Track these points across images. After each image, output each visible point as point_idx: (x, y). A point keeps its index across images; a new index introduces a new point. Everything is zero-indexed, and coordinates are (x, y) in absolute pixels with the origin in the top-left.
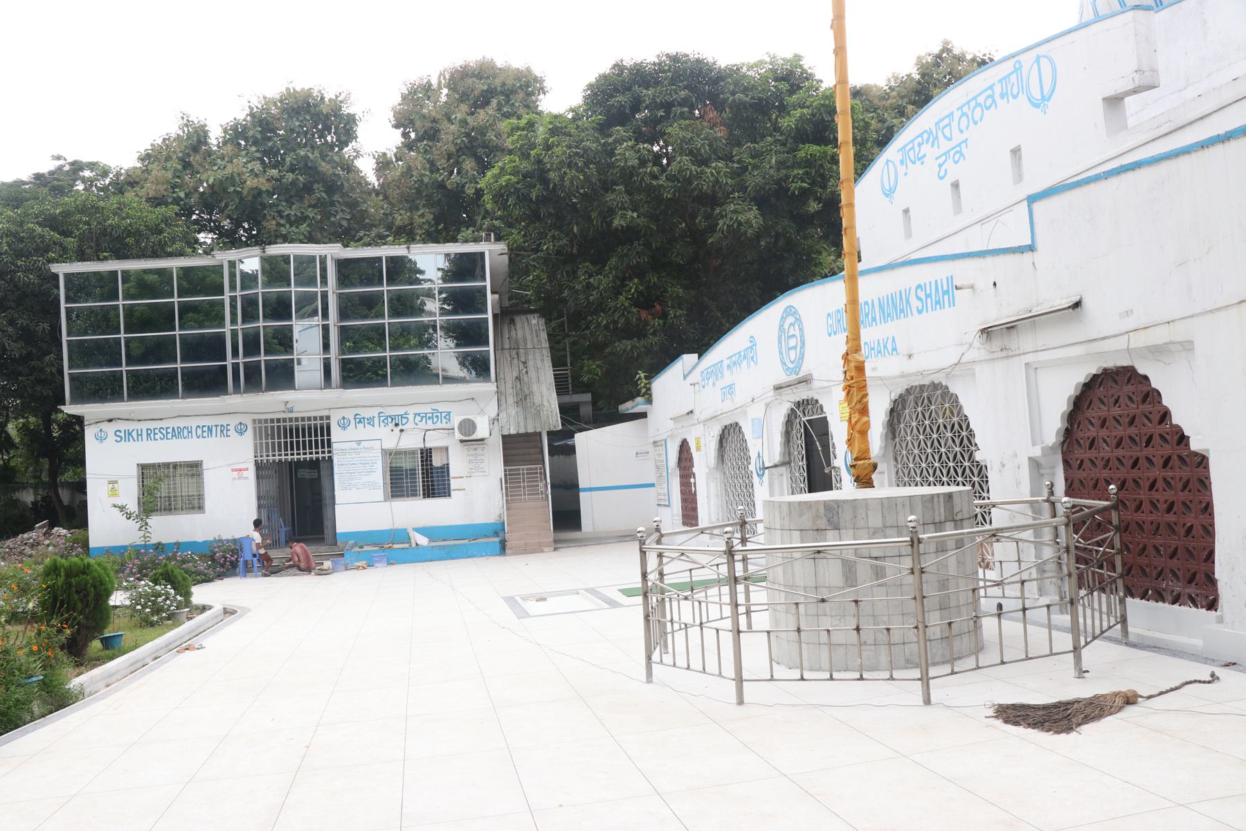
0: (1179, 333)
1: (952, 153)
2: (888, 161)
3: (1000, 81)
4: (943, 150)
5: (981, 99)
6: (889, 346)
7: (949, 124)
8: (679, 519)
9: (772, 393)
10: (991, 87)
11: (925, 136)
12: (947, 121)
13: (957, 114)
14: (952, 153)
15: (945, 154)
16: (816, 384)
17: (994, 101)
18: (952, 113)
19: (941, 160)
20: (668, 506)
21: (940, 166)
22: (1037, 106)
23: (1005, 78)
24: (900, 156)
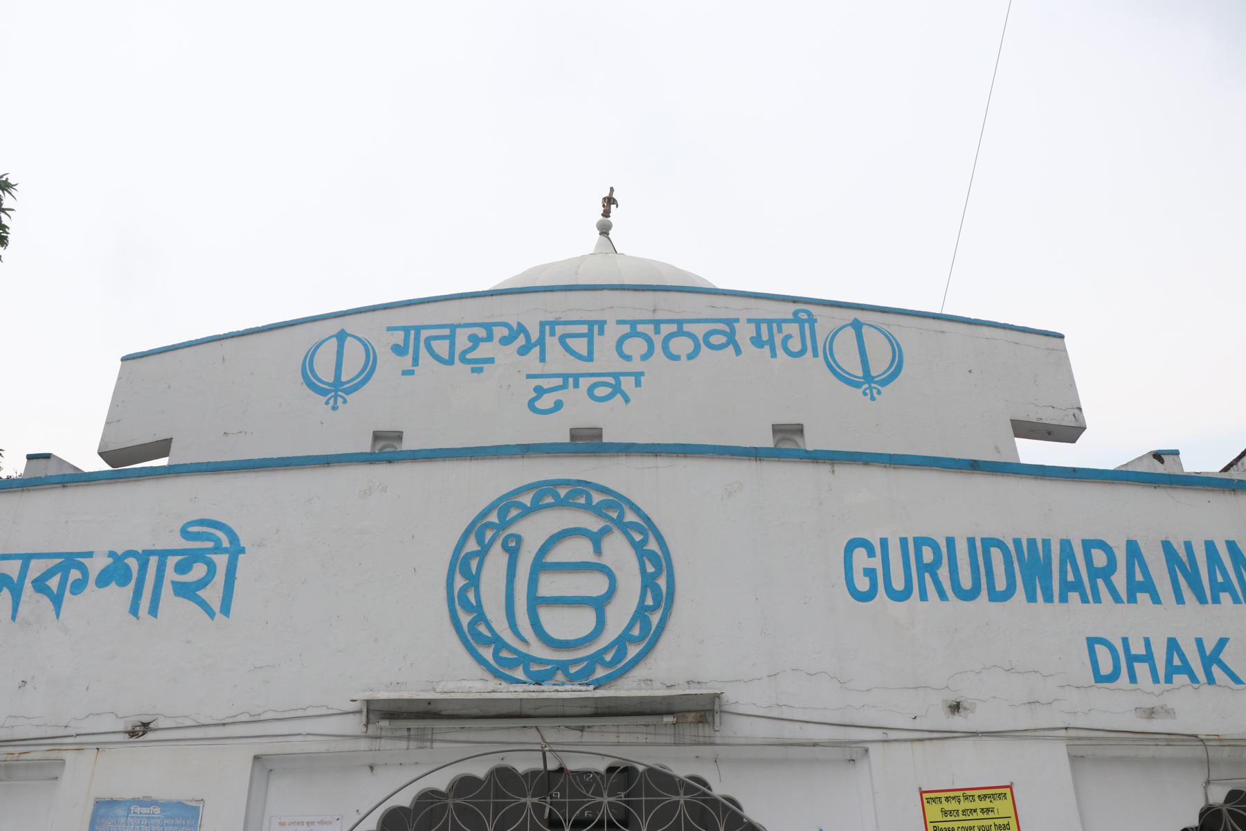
1: (585, 383)
2: (342, 336)
3: (758, 323)
4: (550, 368)
5: (699, 330)
7: (589, 336)
9: (354, 725)
10: (730, 322)
11: (500, 332)
12: (584, 329)
13: (614, 331)
15: (565, 377)
17: (731, 340)
18: (602, 324)
19: (546, 383)
21: (540, 391)
22: (857, 385)
23: (769, 322)
24: (399, 338)
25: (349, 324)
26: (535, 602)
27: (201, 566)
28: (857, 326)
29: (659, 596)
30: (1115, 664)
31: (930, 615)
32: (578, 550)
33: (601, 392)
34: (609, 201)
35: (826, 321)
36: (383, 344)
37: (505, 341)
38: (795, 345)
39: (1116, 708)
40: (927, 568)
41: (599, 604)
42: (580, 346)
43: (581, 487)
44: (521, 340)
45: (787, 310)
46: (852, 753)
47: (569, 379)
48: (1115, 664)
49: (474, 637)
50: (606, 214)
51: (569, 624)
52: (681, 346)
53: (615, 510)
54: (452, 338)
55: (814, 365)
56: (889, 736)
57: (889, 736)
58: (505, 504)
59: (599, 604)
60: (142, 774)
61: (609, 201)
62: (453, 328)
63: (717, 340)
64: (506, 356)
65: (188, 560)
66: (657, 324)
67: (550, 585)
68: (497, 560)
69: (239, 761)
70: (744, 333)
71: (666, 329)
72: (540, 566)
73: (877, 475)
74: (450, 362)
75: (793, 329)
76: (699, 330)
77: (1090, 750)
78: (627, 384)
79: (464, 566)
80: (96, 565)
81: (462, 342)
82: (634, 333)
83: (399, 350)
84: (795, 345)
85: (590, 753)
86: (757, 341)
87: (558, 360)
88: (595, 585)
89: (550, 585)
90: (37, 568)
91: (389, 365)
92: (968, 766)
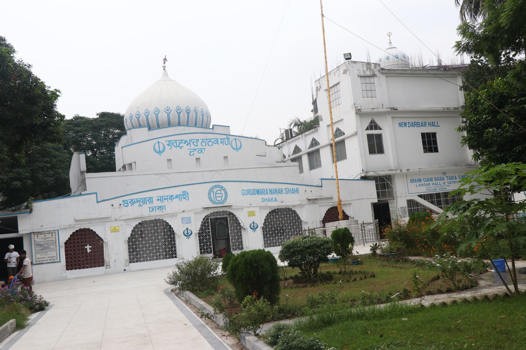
0: (350, 202)
1: (197, 150)
2: (158, 142)
3: (221, 139)
5: (213, 141)
6: (274, 199)
8: (65, 267)
10: (217, 139)
11: (183, 142)
13: (200, 141)
14: (197, 150)
16: (233, 207)
17: (217, 142)
19: (191, 150)
20: (60, 262)
21: (191, 152)
24: (168, 143)
25: (159, 140)
26: (216, 197)
27: (185, 195)
28: (235, 139)
29: (226, 196)
30: (264, 200)
31: (249, 196)
32: (219, 192)
33: (200, 152)
34: (165, 60)
35: (231, 138)
36: (166, 144)
37: (184, 143)
38: (227, 143)
39: (263, 204)
40: (249, 192)
41: (221, 197)
42: (195, 144)
43: (219, 186)
44: (187, 143)
45: (225, 137)
46: (242, 209)
47: (195, 150)
48: (264, 200)
49: (211, 201)
50: (164, 63)
51: (219, 199)
52: (210, 143)
53: (222, 187)
54: (176, 142)
55: (229, 146)
56: (245, 207)
57: (245, 207)
58: (212, 188)
59: (221, 197)
60: (185, 215)
61: (165, 60)
62: (176, 141)
63: (216, 142)
64: (185, 146)
65: (184, 195)
66: (207, 139)
67: (217, 195)
68: (212, 193)
69: (193, 213)
70: (219, 141)
71: (208, 140)
72: (216, 194)
73: (245, 183)
74: (176, 147)
75: (226, 140)
76: (213, 141)
77: (261, 208)
78: (203, 150)
79: (209, 194)
80: (175, 196)
81: (178, 144)
82: (203, 141)
83: (168, 145)
84: (227, 143)
85: (221, 210)
86: (221, 142)
87: (193, 147)
88: (221, 195)
89: (217, 195)
90: (169, 197)
91: (167, 148)
92: (251, 209)
